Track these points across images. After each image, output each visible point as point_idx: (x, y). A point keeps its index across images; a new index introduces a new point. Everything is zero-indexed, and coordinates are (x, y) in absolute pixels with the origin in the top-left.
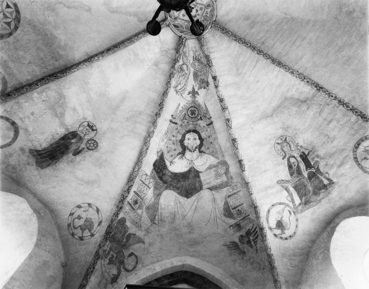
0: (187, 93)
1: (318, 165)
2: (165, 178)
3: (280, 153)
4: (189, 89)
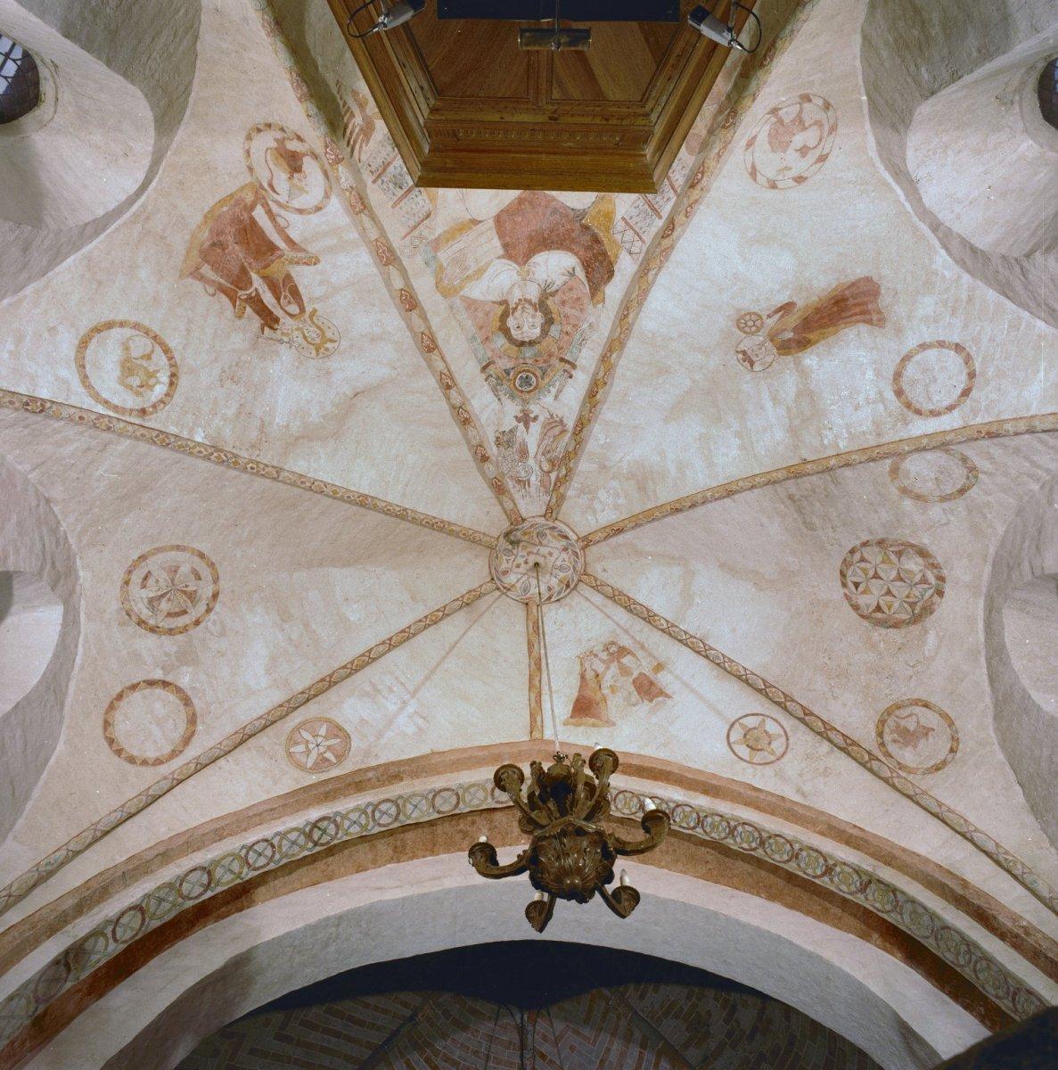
0: (541, 418)
1: (235, 307)
2: (586, 238)
3: (325, 321)
4: (536, 428)
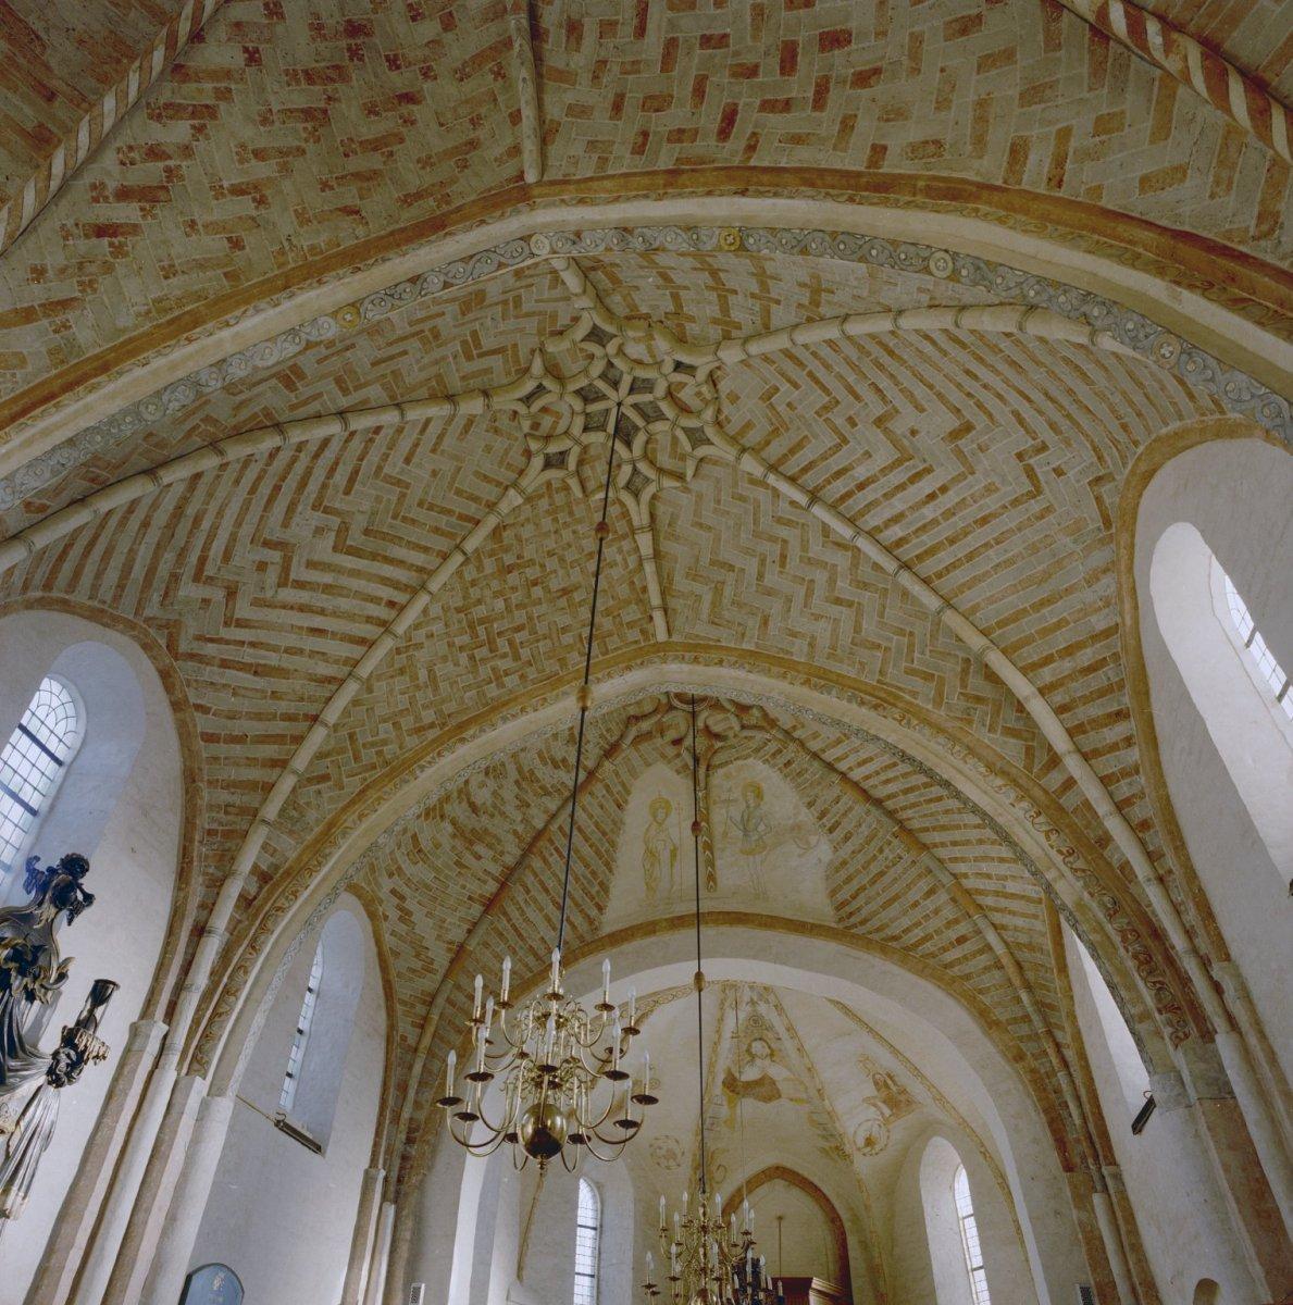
4: (746, 999)
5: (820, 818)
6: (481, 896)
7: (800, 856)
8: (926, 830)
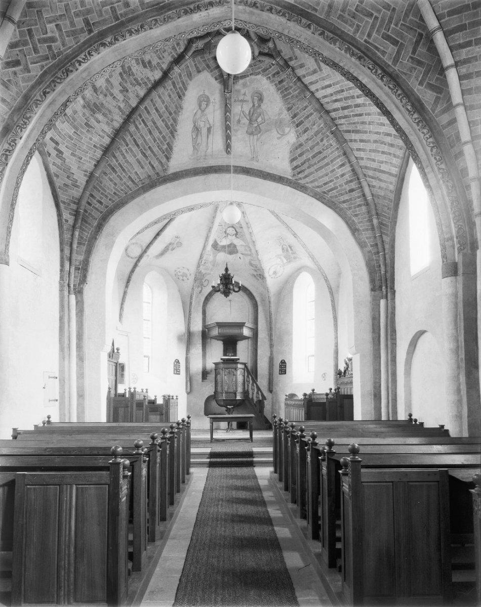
5: (293, 118)
6: (101, 145)
7: (278, 138)
8: (349, 131)
